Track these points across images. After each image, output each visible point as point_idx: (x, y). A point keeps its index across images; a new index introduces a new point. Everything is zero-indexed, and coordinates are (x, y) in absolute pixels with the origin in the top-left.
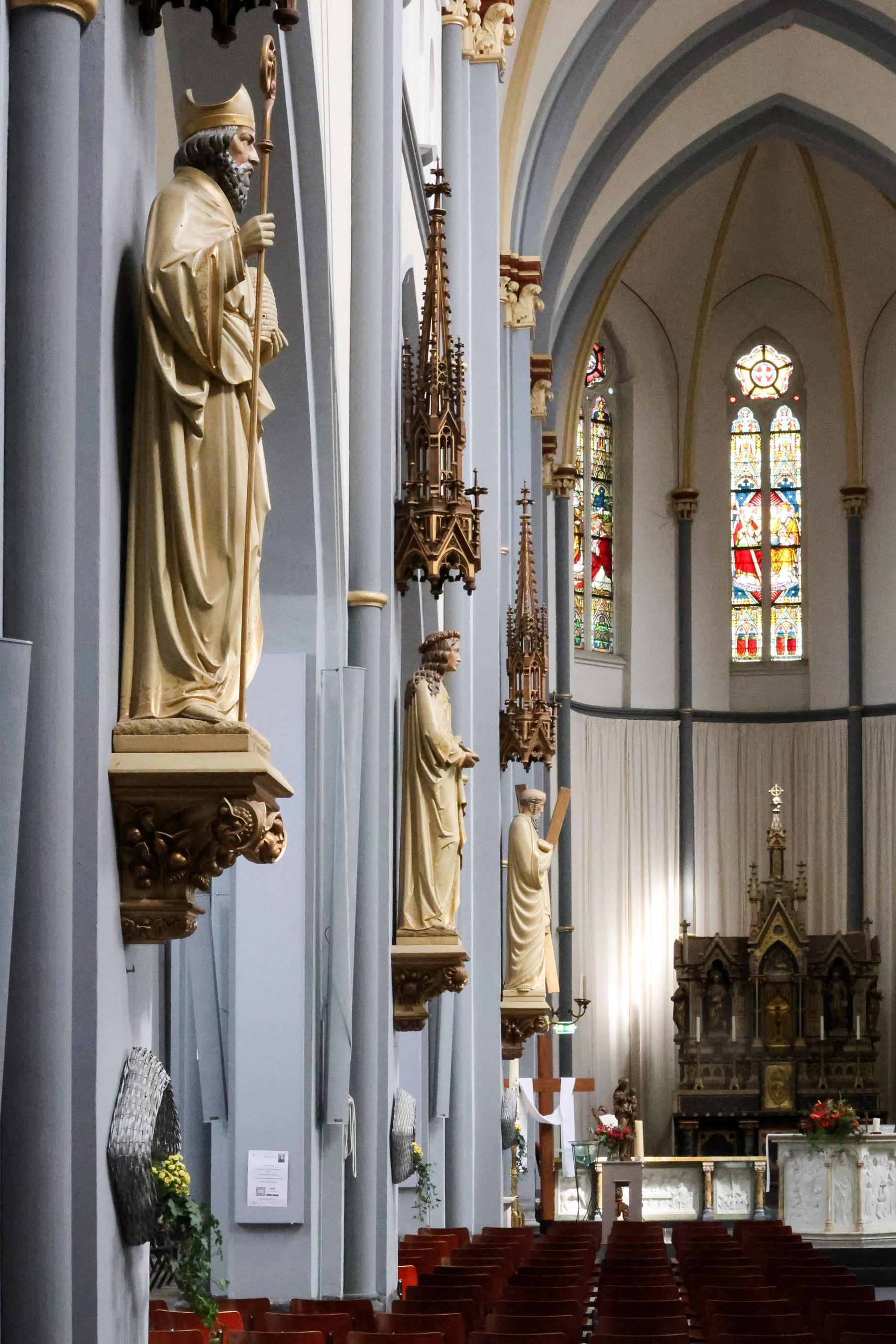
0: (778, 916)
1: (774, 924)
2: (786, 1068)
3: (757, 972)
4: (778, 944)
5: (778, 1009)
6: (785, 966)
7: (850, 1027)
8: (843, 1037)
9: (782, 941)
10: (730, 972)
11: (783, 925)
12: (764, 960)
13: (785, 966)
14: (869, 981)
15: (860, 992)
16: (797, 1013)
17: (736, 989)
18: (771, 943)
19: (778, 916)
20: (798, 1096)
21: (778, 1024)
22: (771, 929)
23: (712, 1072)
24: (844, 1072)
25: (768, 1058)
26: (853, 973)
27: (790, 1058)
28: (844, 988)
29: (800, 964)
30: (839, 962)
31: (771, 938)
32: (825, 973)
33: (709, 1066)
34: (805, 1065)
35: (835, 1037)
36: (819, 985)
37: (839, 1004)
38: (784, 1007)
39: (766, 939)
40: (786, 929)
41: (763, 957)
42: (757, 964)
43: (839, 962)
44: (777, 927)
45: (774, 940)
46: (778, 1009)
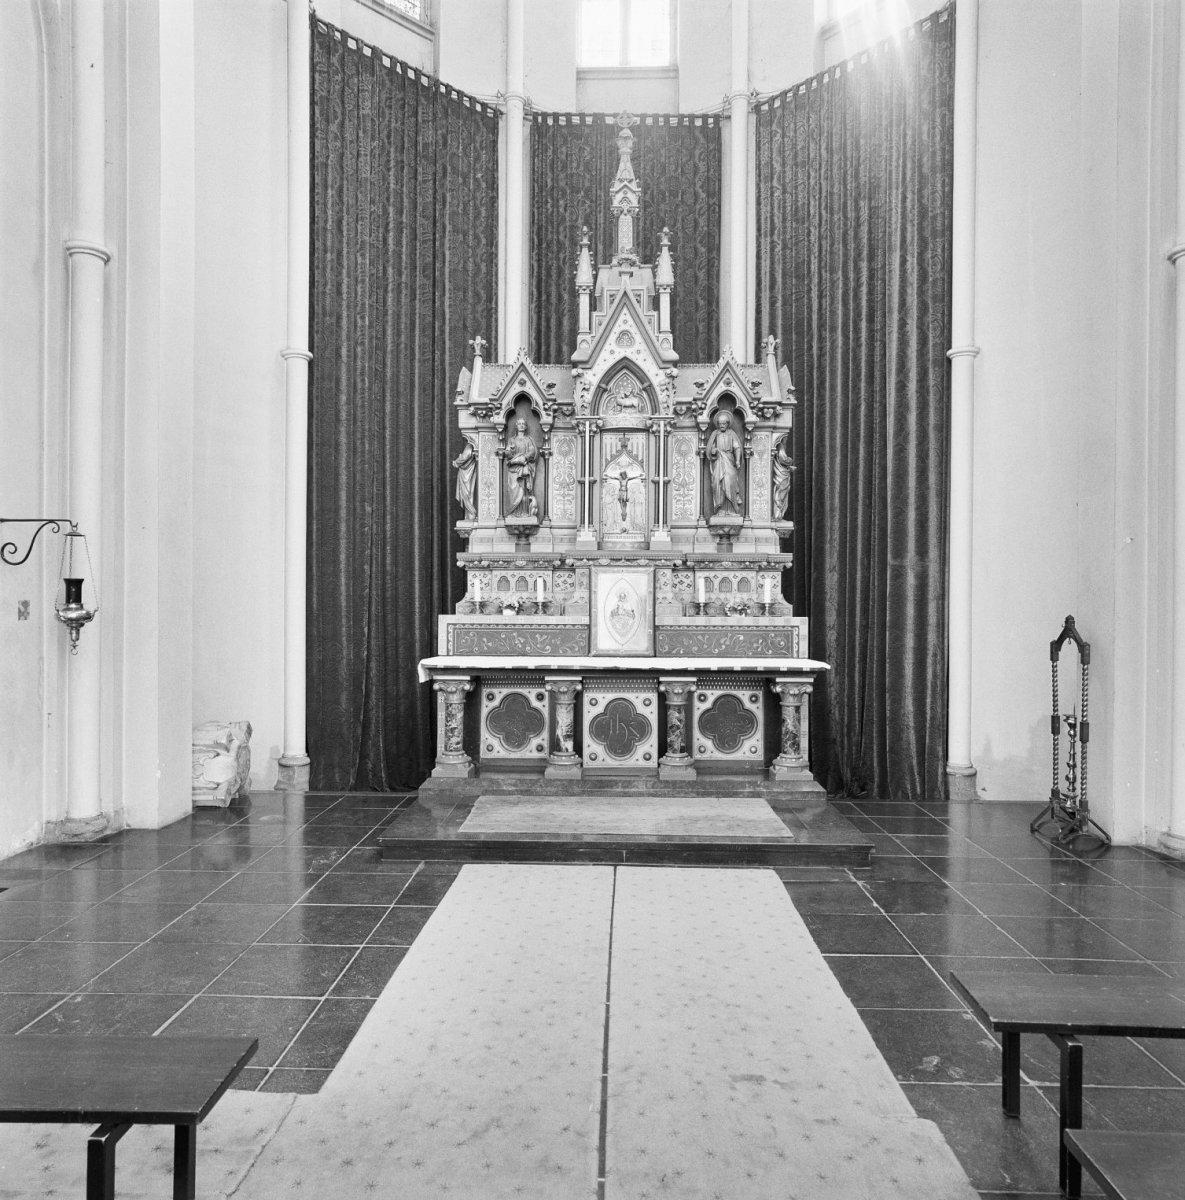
0: (625, 315)
1: (617, 330)
2: (636, 582)
3: (587, 411)
4: (625, 365)
5: (623, 475)
6: (635, 401)
7: (744, 510)
8: (732, 527)
9: (633, 357)
10: (543, 413)
11: (634, 330)
12: (601, 391)
13: (635, 401)
14: (776, 435)
15: (761, 454)
16: (657, 483)
17: (556, 442)
18: (612, 361)
19: (625, 315)
20: (656, 628)
21: (624, 502)
22: (613, 337)
23: (513, 581)
24: (735, 586)
25: (604, 561)
26: (751, 417)
27: (643, 562)
28: (736, 444)
29: (662, 397)
30: (727, 399)
31: (612, 352)
32: (704, 418)
33: (508, 574)
34: (668, 572)
35: (722, 527)
36: (692, 440)
37: (724, 470)
38: (634, 471)
39: (604, 354)
40: (638, 338)
41: (599, 387)
42: (589, 397)
43: (727, 399)
44: (624, 333)
45: (618, 357)
46: (623, 475)
